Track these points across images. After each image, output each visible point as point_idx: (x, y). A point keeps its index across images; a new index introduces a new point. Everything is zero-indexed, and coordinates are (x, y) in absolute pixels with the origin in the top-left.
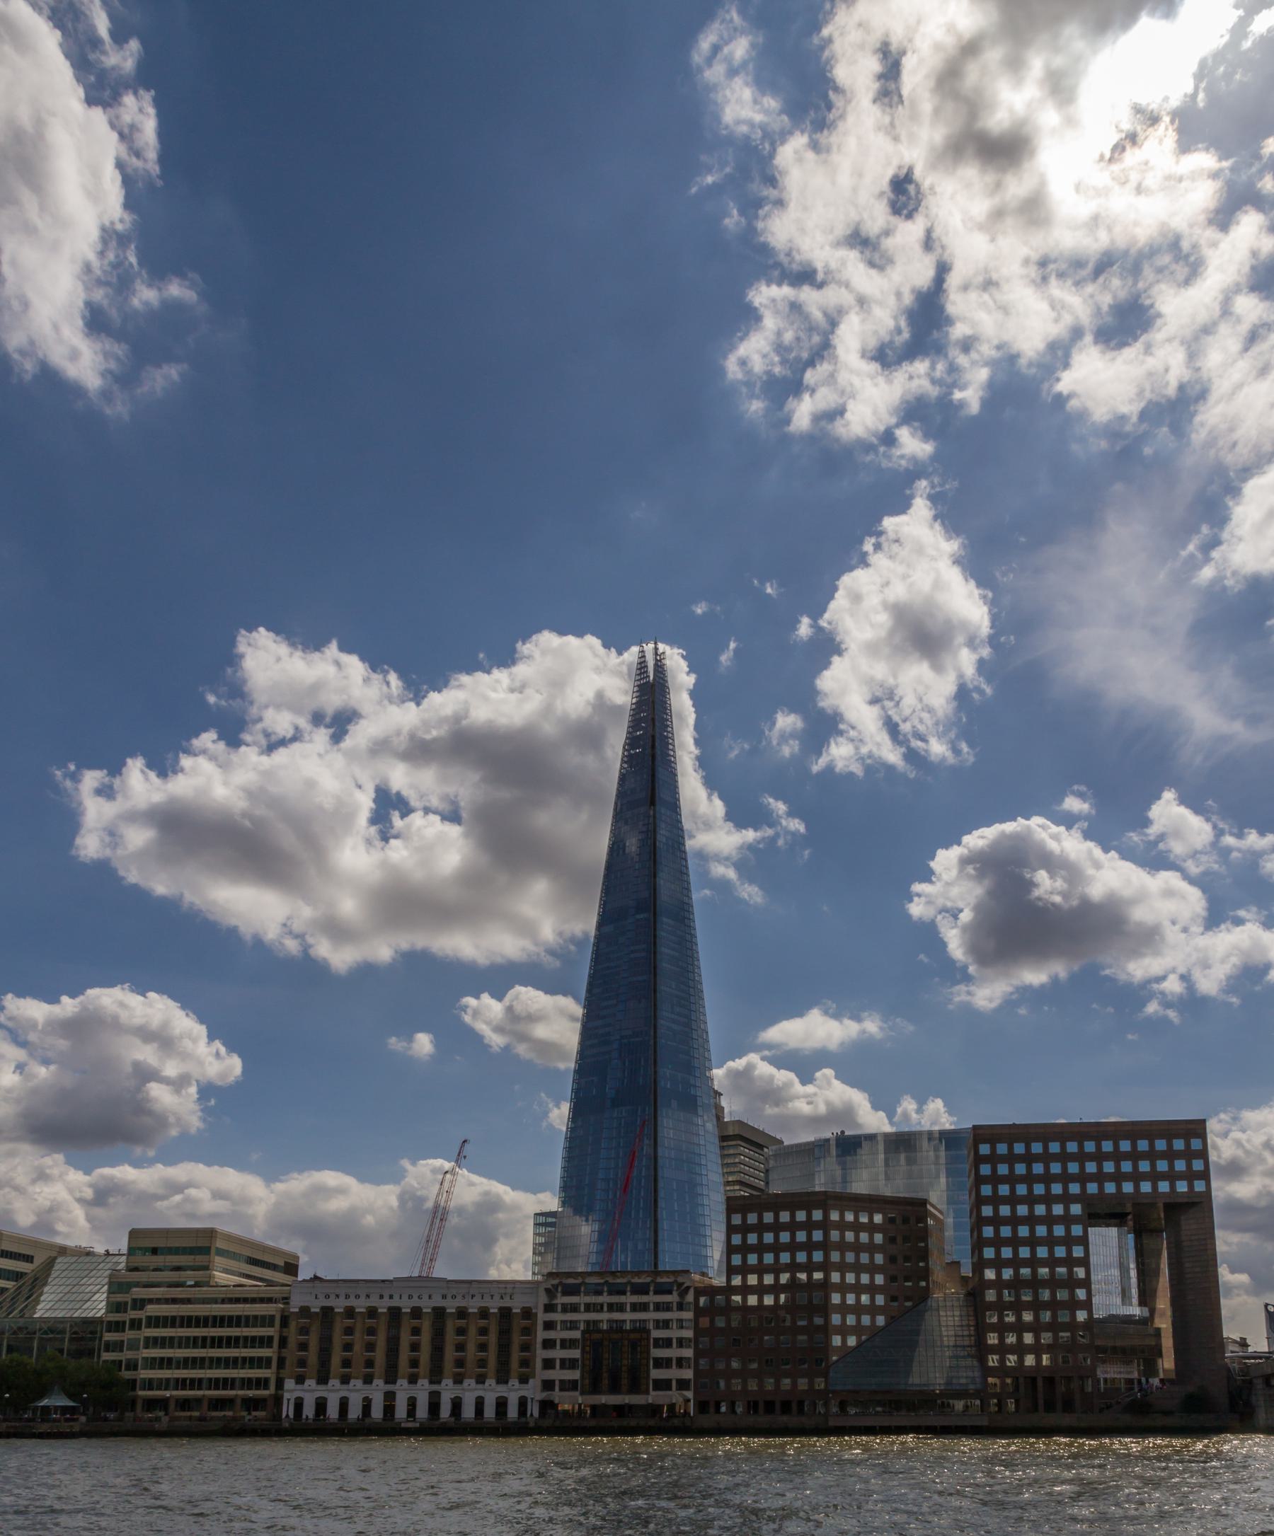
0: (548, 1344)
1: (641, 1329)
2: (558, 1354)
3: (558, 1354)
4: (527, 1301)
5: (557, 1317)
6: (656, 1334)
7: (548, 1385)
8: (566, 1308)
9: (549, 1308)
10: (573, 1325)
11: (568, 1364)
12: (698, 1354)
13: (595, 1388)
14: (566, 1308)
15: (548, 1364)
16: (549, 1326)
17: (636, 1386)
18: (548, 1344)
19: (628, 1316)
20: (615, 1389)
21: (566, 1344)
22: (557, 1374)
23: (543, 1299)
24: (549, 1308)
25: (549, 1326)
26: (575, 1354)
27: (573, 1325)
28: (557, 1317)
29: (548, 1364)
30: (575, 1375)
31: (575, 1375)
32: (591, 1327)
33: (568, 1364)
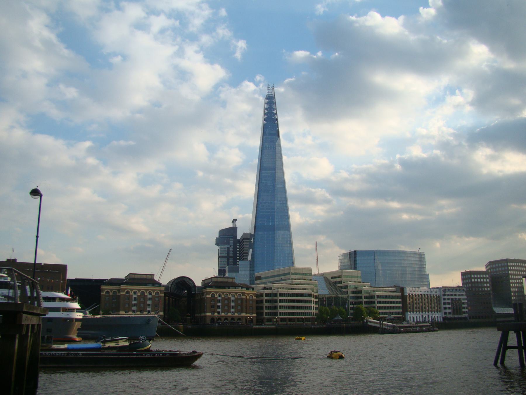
0: (445, 304)
1: (460, 299)
2: (447, 306)
3: (447, 306)
4: (438, 293)
5: (446, 297)
6: (463, 301)
7: (445, 313)
8: (448, 295)
9: (444, 295)
10: (448, 299)
11: (449, 308)
12: (469, 306)
13: (454, 314)
14: (448, 295)
15: (445, 308)
16: (444, 299)
17: (460, 314)
18: (445, 304)
19: (458, 297)
20: (457, 314)
21: (449, 303)
22: (448, 311)
23: (442, 293)
24: (444, 295)
25: (444, 299)
26: (450, 306)
27: (448, 299)
28: (446, 297)
29: (445, 308)
30: (450, 311)
31: (450, 311)
32: (452, 299)
33: (449, 308)
